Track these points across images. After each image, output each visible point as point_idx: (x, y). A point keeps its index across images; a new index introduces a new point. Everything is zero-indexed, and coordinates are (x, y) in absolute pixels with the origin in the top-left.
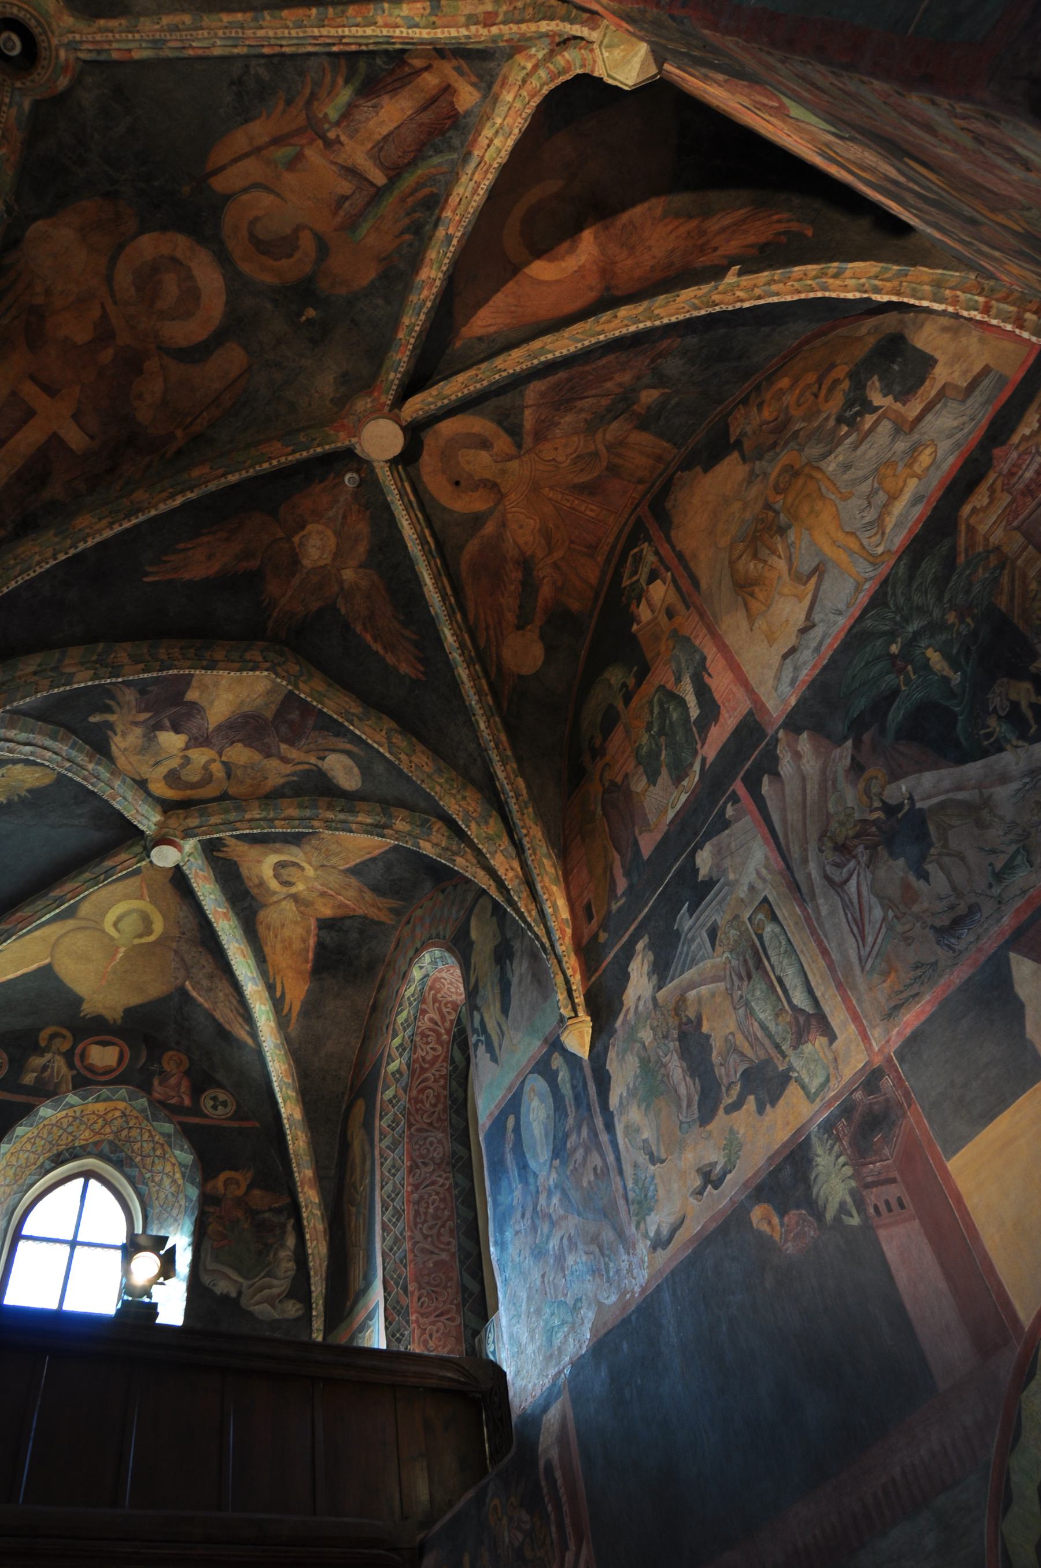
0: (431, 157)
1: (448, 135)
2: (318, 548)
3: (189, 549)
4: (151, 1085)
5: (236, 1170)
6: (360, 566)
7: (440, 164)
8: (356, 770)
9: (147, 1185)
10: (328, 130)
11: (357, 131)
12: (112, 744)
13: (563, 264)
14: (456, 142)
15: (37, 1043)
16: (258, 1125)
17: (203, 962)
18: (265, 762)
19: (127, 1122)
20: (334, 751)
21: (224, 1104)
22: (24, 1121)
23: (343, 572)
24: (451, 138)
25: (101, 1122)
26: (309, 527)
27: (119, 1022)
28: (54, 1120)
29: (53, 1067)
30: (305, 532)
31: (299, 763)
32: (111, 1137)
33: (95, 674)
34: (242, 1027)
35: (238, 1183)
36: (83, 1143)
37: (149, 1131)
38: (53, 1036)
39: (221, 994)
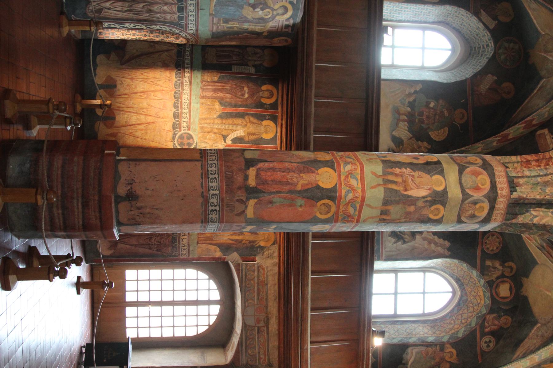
4: (493, 313)
5: (457, 356)
9: (450, 318)
15: (506, 262)
16: (480, 362)
17: (548, 333)
19: (476, 305)
21: (488, 346)
22: (469, 266)
25: (475, 294)
27: (522, 294)
28: (472, 276)
29: (495, 271)
32: (469, 300)
34: (521, 352)
35: (451, 357)
36: (466, 288)
37: (472, 316)
38: (511, 268)
39: (535, 341)
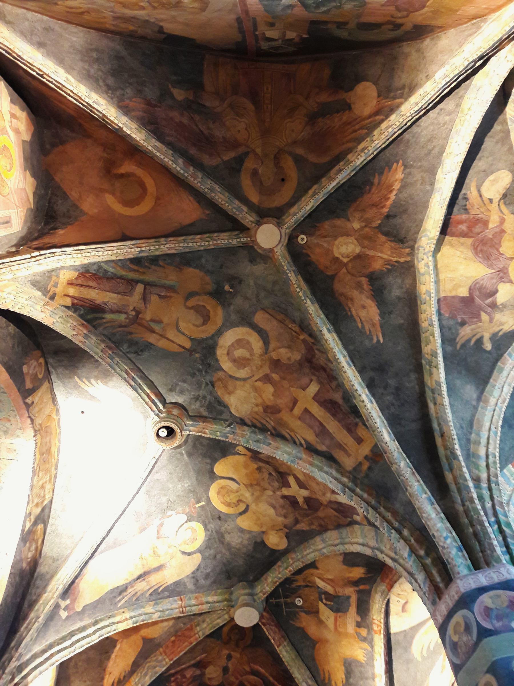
0: (112, 273)
1: (94, 272)
2: (348, 246)
3: (361, 320)
6: (349, 220)
7: (113, 267)
8: (491, 177)
10: (132, 315)
11: (123, 305)
12: (511, 329)
13: (142, 176)
14: (95, 267)
18: (509, 232)
20: (481, 196)
23: (356, 229)
24: (95, 270)
26: (337, 255)
30: (340, 257)
31: (502, 212)
33: (435, 367)
